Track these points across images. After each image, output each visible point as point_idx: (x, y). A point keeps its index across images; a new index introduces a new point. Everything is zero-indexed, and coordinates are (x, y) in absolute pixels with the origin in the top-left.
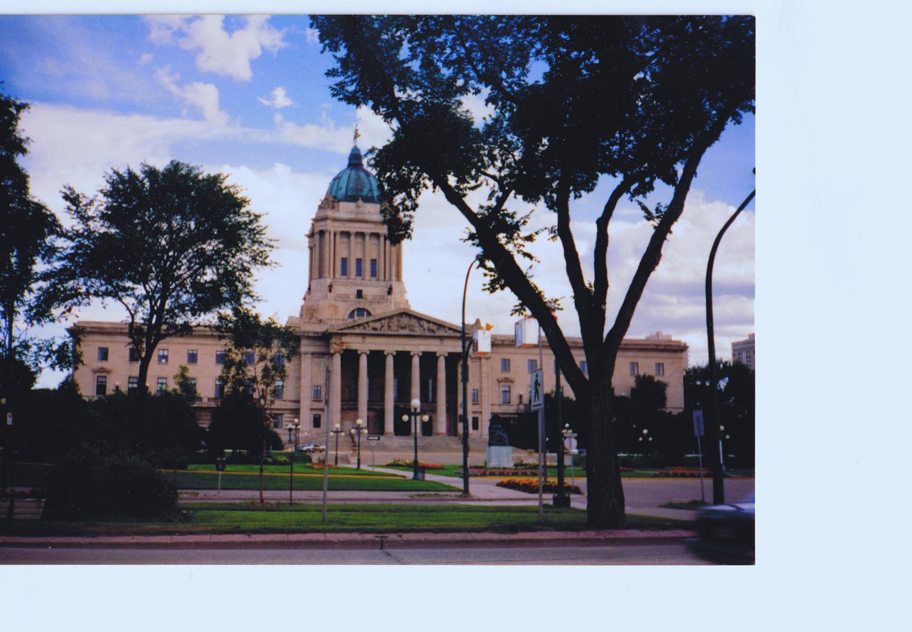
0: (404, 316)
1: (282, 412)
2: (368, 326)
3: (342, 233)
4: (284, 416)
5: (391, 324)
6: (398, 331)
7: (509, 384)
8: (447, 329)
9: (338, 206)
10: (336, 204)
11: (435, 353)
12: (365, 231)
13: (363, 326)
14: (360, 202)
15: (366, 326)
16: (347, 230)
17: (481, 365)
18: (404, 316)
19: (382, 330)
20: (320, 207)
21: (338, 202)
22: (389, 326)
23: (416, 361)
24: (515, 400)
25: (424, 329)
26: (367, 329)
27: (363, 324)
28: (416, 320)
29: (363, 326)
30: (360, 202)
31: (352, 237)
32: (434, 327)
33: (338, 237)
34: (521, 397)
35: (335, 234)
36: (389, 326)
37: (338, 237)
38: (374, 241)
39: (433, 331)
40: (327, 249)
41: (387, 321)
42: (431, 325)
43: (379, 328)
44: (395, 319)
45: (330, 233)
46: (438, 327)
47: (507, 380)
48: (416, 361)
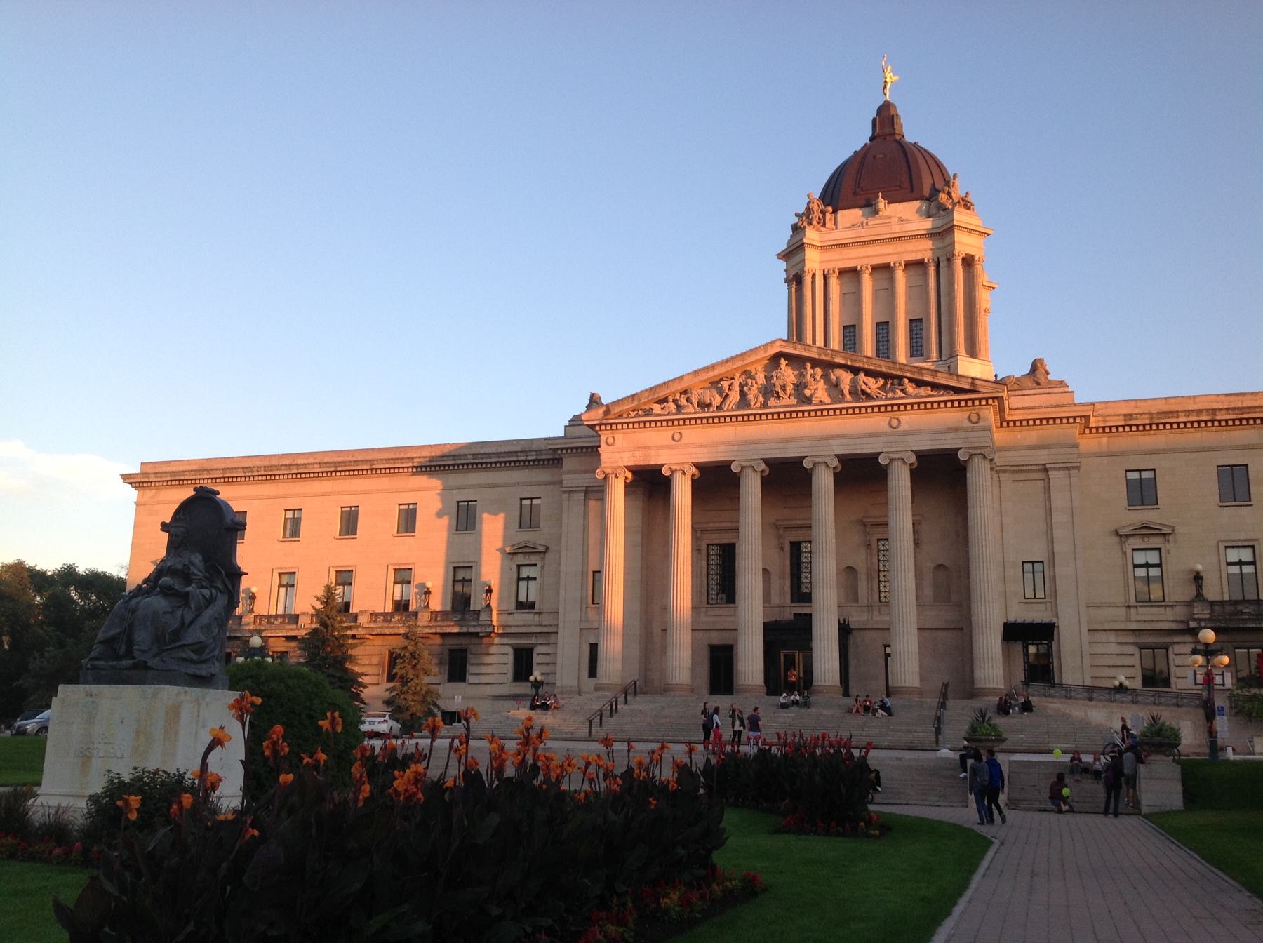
0: (783, 362)
1: (533, 641)
4: (537, 650)
6: (765, 405)
7: (1156, 542)
11: (874, 457)
12: (891, 260)
13: (675, 401)
16: (851, 264)
17: (1048, 490)
18: (783, 362)
23: (824, 482)
24: (1179, 591)
34: (1198, 578)
35: (825, 278)
37: (834, 282)
46: (881, 382)
47: (1146, 530)
48: (824, 482)
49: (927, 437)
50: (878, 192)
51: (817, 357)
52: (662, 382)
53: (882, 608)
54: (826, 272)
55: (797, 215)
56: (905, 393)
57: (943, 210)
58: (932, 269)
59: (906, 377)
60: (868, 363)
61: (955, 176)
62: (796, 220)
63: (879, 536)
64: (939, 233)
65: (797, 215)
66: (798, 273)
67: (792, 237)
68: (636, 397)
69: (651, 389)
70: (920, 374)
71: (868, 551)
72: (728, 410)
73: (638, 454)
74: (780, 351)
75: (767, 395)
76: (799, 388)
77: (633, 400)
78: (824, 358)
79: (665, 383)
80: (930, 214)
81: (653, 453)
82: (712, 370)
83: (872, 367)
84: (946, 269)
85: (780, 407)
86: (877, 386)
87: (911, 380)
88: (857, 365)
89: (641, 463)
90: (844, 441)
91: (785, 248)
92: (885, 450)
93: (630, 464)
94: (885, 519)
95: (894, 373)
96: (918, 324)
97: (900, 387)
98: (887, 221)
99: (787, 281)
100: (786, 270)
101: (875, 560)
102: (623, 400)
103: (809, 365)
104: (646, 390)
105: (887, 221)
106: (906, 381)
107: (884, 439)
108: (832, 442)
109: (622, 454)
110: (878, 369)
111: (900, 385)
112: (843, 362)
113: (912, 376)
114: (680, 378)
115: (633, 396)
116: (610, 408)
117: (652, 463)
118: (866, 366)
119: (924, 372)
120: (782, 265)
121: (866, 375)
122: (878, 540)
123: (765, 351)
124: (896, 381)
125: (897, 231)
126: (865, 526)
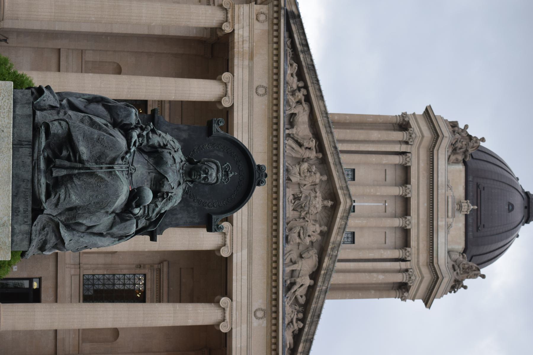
0: (329, 203)
2: (299, 102)
3: (406, 169)
5: (305, 166)
8: (297, 326)
9: (457, 162)
10: (460, 158)
11: (227, 292)
13: (299, 89)
14: (468, 207)
15: (300, 95)
18: (329, 203)
19: (290, 142)
20: (454, 125)
21: (465, 163)
22: (301, 161)
25: (293, 262)
26: (293, 100)
27: (306, 87)
28: (316, 237)
29: (299, 89)
30: (468, 207)
31: (397, 191)
32: (300, 292)
33: (397, 160)
36: (301, 161)
37: (397, 160)
38: (393, 238)
39: (288, 288)
40: (375, 135)
41: (313, 155)
42: (308, 282)
43: (294, 131)
44: (317, 178)
45: (407, 143)
46: (302, 301)
49: (244, 344)
50: (477, 206)
51: (332, 239)
52: (320, 77)
53: (78, 277)
54: (409, 155)
55: (466, 127)
56: (288, 324)
57: (453, 266)
58: (397, 254)
59: (304, 327)
60: (320, 291)
61: (483, 276)
62: (461, 126)
63: (148, 277)
64: (433, 263)
65: (466, 127)
66: (411, 127)
67: (446, 121)
68: (305, 48)
69: (313, 66)
70: (306, 341)
71: (134, 266)
72: (285, 144)
73: (246, 45)
74: (340, 203)
75: (297, 186)
76: (302, 220)
77: (302, 45)
78: (330, 247)
79: (318, 81)
80: (451, 253)
81: (246, 62)
82: (327, 132)
83: (316, 294)
84: (398, 268)
85: (284, 202)
86: (299, 297)
87: (301, 330)
88: (321, 279)
89: (236, 50)
90: (245, 264)
91: (436, 114)
92: (234, 303)
93: (236, 36)
94: (165, 297)
95: (310, 315)
96: (350, 240)
97: (294, 320)
98: (450, 214)
99: (404, 115)
100: (414, 114)
101: (125, 272)
102: (304, 34)
103: (325, 229)
104: (312, 60)
105: (450, 214)
106: (301, 325)
107: (245, 301)
108: (245, 252)
109: (247, 29)
110: (314, 300)
111: (298, 320)
112: (325, 265)
113: (305, 333)
114: (321, 97)
115: (307, 45)
116: (297, 20)
117: (236, 61)
118: (318, 289)
119: (308, 344)
120: (420, 111)
121: (309, 287)
122: (145, 275)
123: (342, 188)
124: (301, 316)
125: (440, 223)
126: (160, 263)
